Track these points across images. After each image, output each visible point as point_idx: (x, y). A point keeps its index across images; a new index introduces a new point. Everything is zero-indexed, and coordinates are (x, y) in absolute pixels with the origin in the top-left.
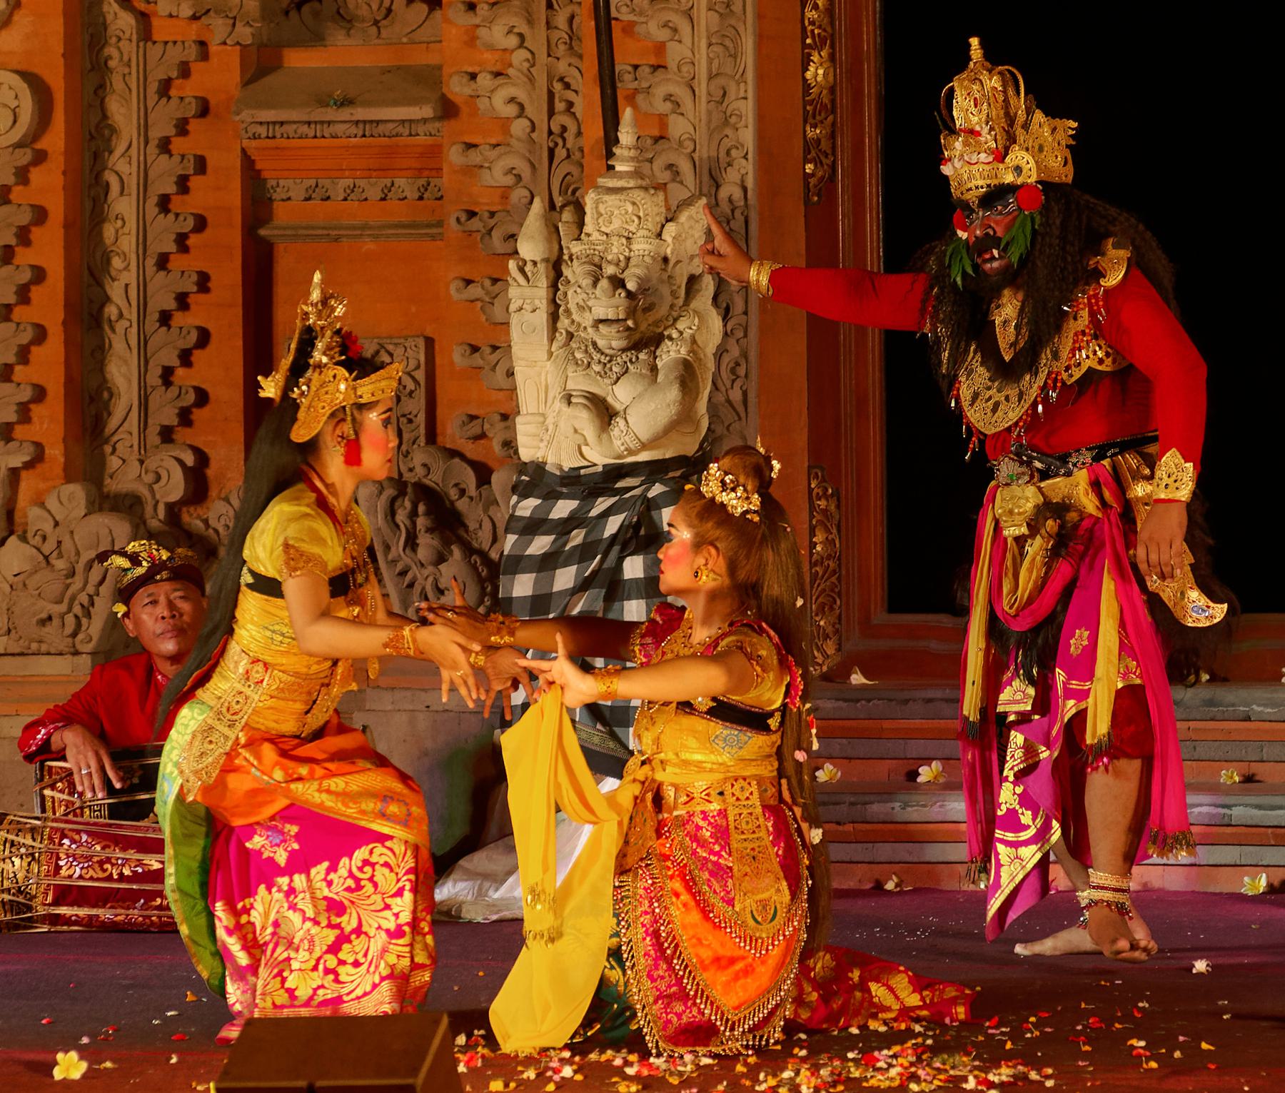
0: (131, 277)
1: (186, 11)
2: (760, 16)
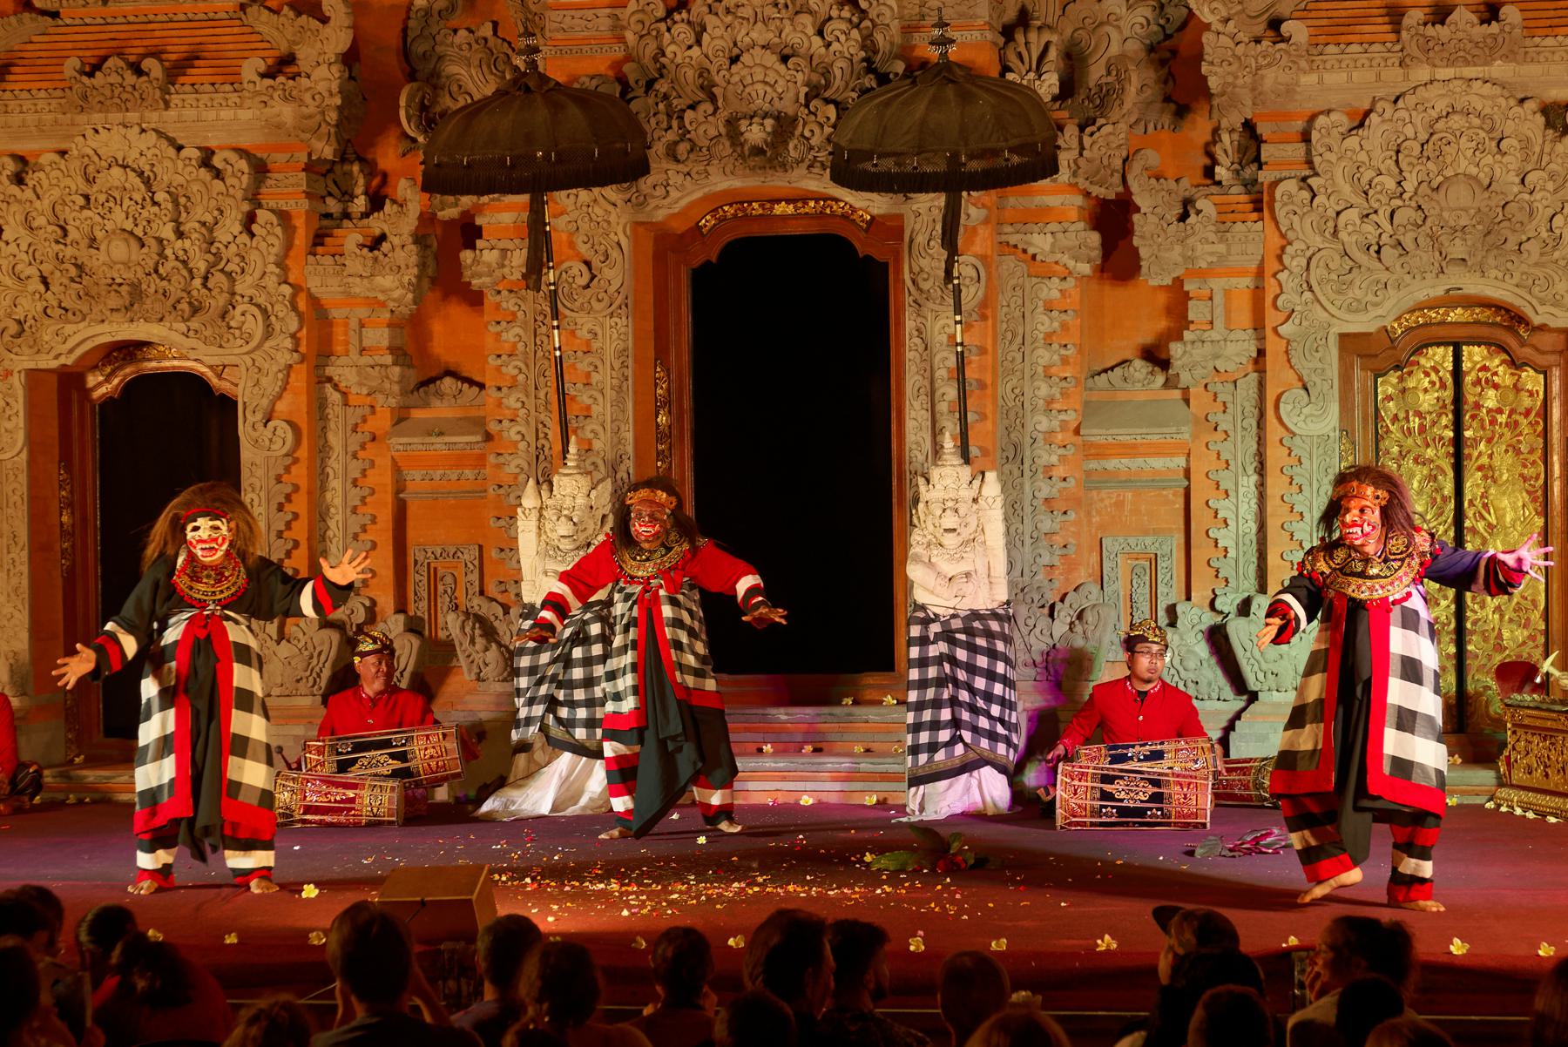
0: (339, 517)
1: (365, 391)
2: (635, 393)
